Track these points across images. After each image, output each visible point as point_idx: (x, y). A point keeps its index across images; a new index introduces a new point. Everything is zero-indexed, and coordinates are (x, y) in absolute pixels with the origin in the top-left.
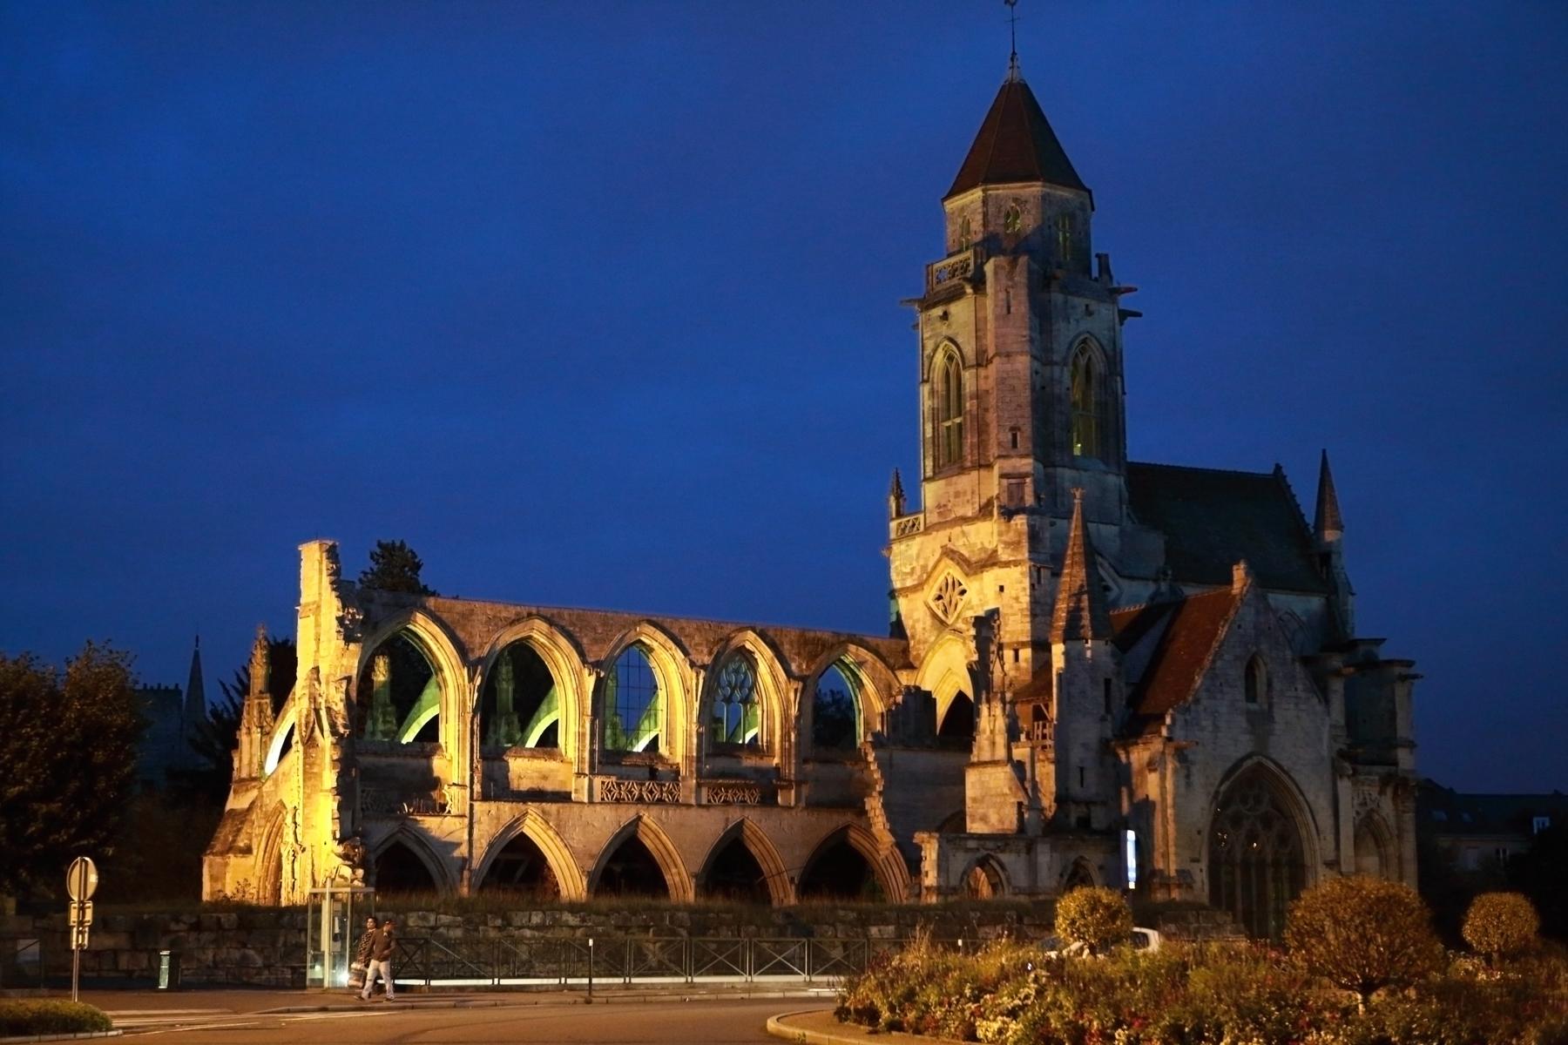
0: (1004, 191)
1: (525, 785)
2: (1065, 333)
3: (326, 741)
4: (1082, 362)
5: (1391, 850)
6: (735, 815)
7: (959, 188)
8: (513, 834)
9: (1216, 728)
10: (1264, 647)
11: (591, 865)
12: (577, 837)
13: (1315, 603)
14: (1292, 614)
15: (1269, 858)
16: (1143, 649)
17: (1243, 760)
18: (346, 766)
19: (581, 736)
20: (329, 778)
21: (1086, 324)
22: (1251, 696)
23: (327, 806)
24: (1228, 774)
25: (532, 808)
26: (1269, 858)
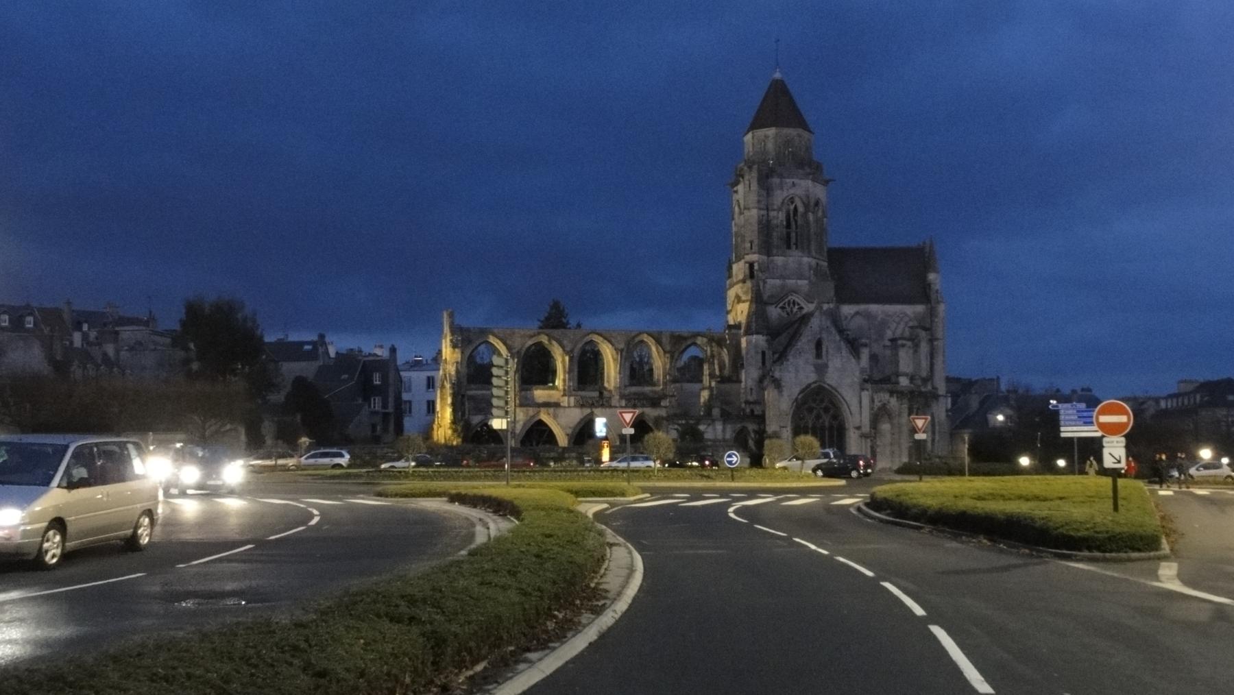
0: (761, 133)
1: (540, 400)
2: (779, 197)
3: (448, 386)
4: (792, 207)
5: (895, 421)
6: (637, 411)
7: (756, 124)
8: (536, 419)
9: (797, 371)
10: (824, 335)
11: (570, 431)
12: (563, 421)
13: (920, 308)
14: (906, 315)
15: (827, 424)
16: (783, 339)
17: (810, 385)
18: (454, 396)
19: (564, 380)
20: (449, 400)
21: (792, 191)
22: (819, 355)
23: (449, 411)
24: (802, 392)
25: (542, 410)
26: (827, 424)
